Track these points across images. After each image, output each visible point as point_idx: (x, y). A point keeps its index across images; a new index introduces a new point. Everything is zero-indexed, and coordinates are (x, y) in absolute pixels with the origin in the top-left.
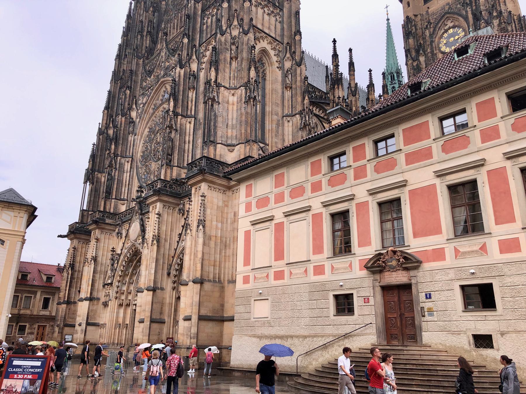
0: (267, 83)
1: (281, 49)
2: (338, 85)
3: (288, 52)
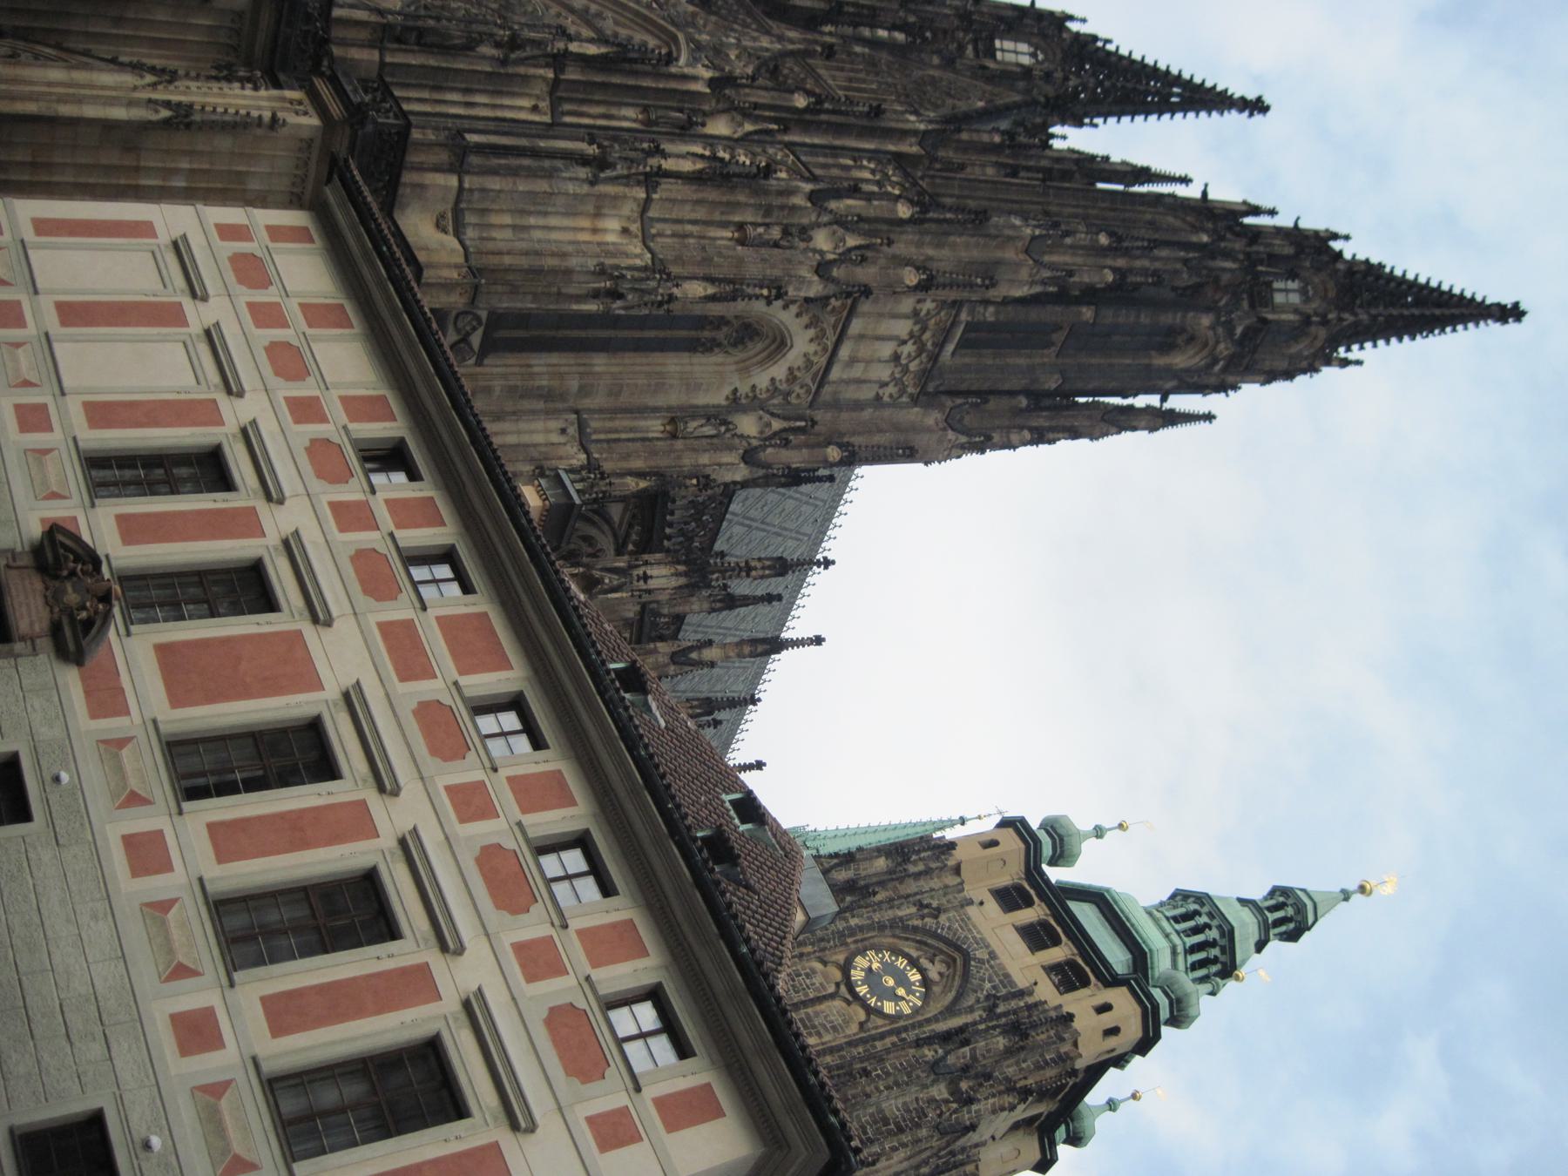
0: (685, 358)
2: (686, 574)
3: (785, 424)
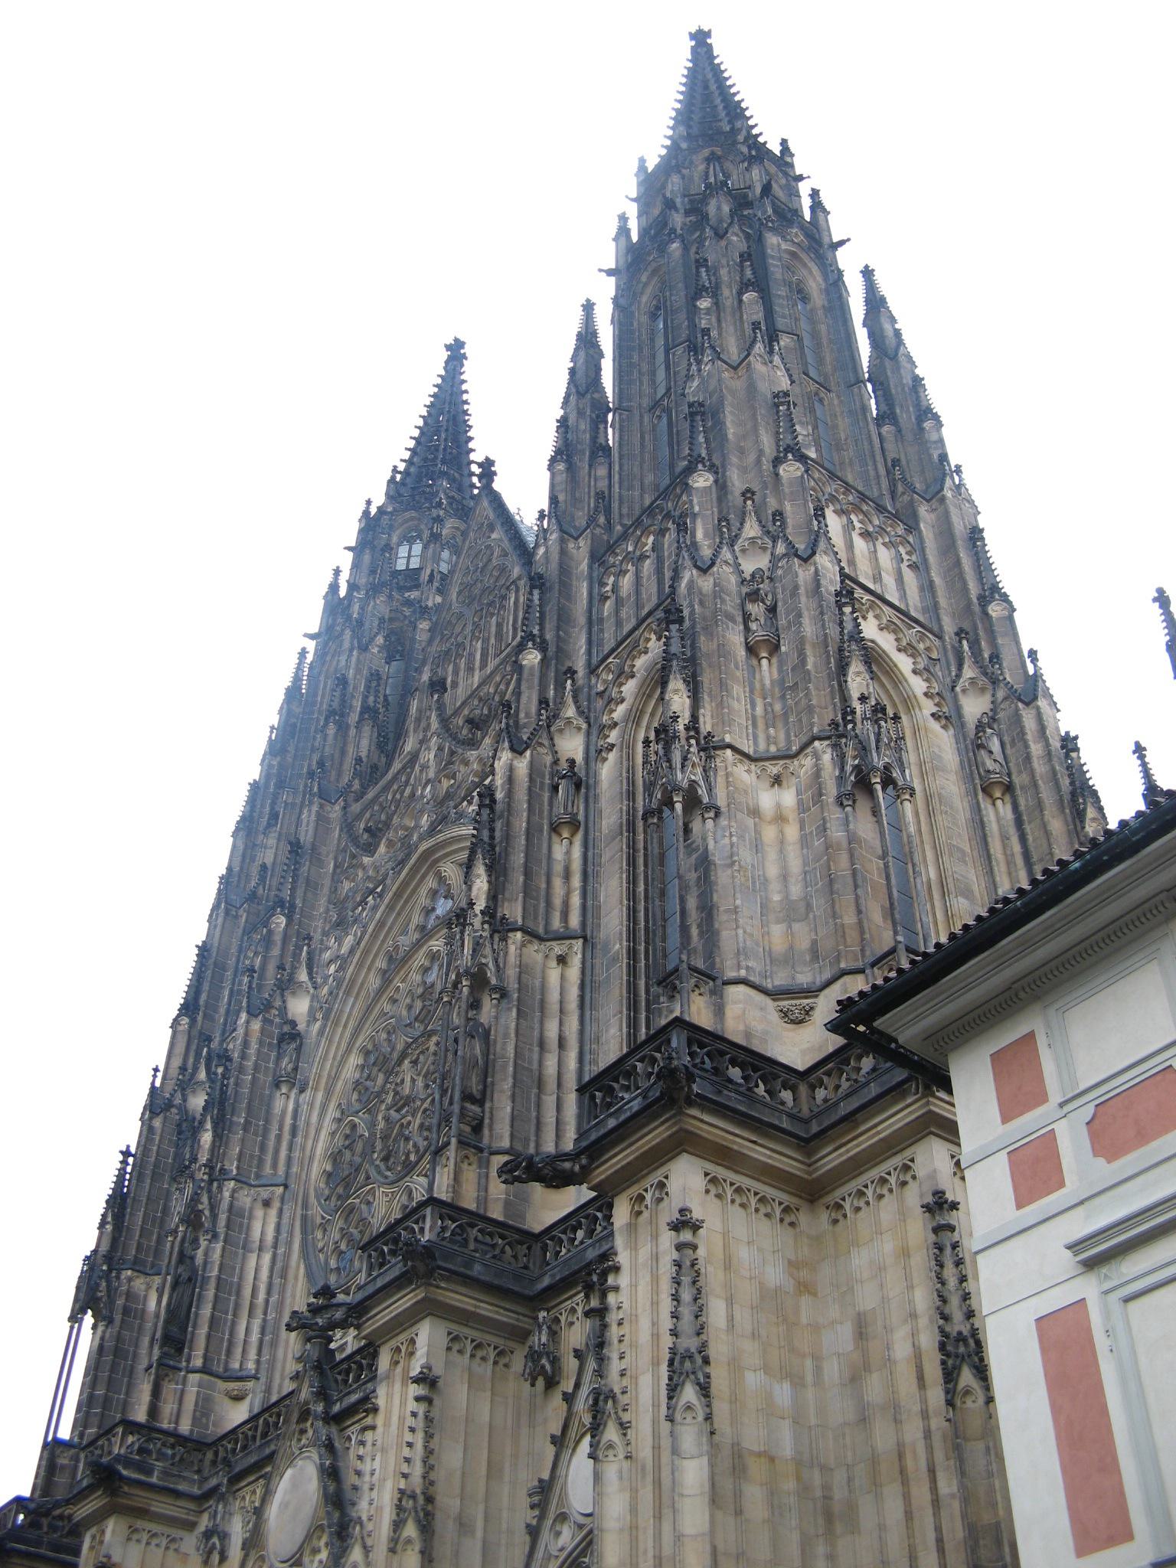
1: (935, 656)
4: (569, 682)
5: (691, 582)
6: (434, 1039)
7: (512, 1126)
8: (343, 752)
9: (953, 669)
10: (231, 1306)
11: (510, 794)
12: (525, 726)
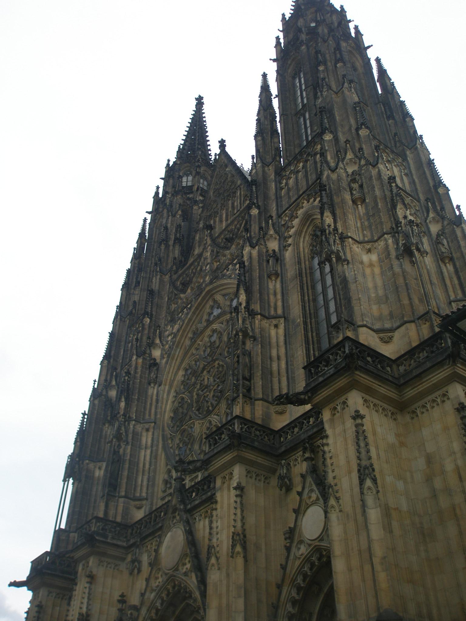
4: (270, 221)
5: (328, 176)
6: (217, 362)
7: (262, 389)
8: (168, 256)
9: (425, 213)
10: (135, 471)
11: (251, 263)
12: (254, 237)
